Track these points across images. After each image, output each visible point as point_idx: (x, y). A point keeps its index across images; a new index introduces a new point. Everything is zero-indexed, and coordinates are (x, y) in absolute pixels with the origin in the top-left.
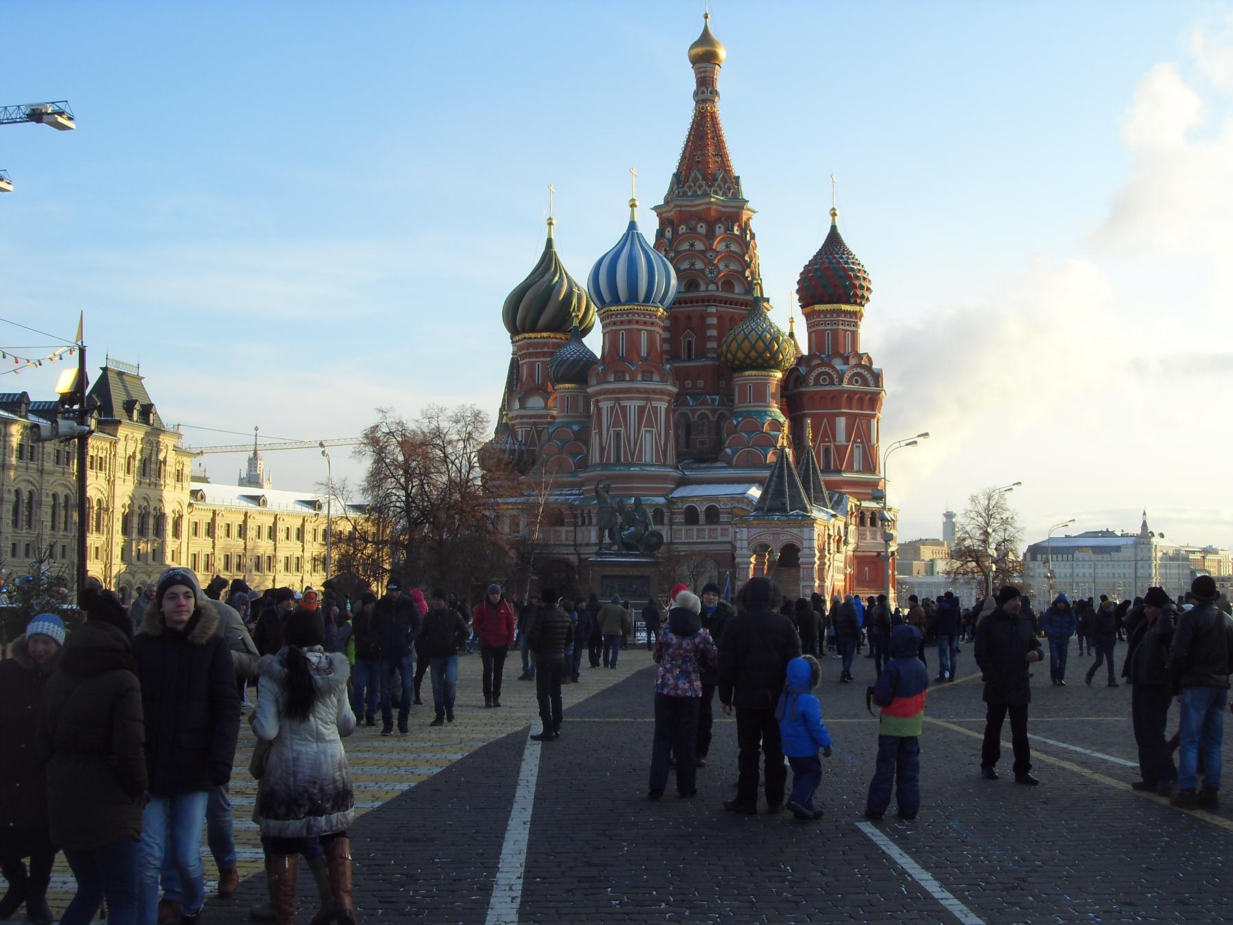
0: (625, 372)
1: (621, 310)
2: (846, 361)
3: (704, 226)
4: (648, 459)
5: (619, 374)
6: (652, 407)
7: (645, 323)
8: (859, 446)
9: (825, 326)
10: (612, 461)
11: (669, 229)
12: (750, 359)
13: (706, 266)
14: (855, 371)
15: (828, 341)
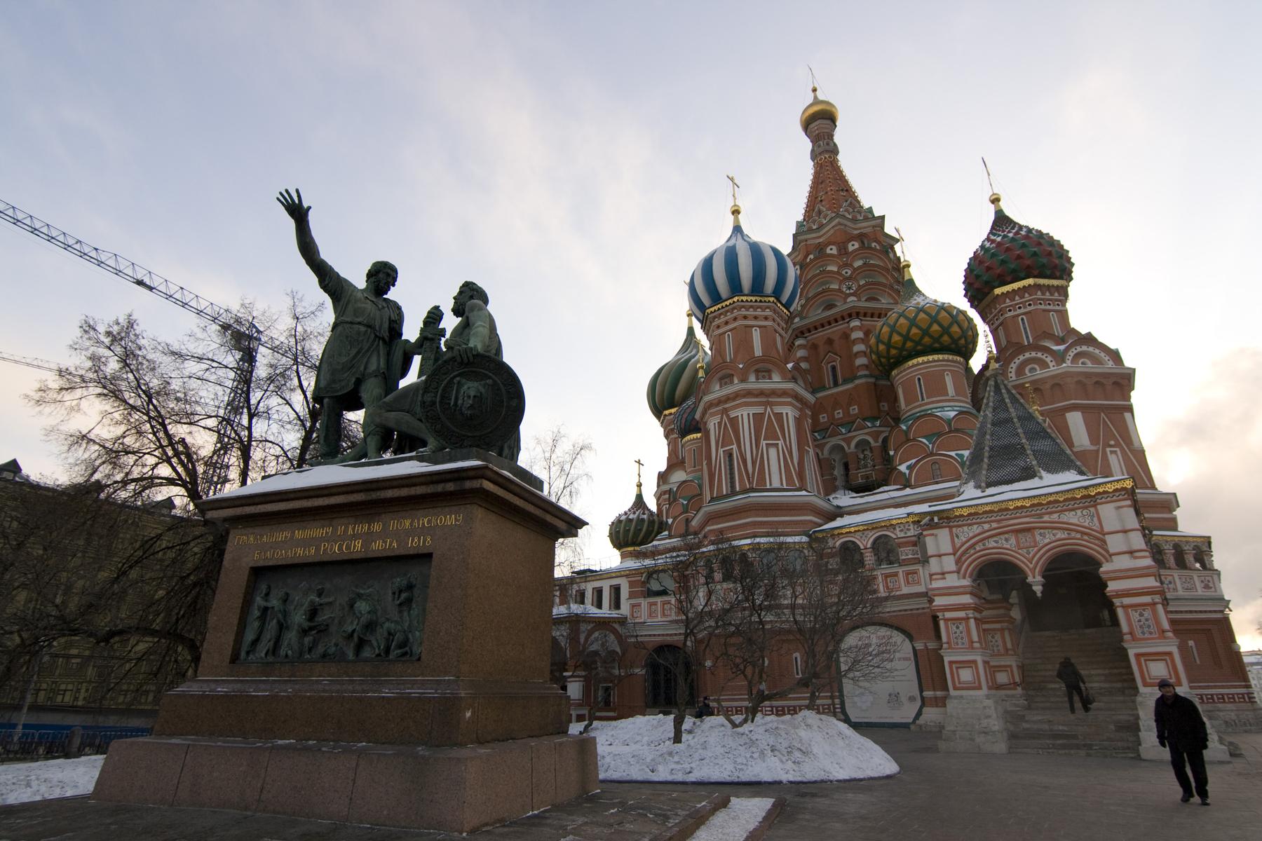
0: (733, 375)
1: (723, 307)
2: (1061, 341)
3: (834, 247)
4: (776, 484)
5: (726, 380)
6: (772, 412)
7: (756, 318)
8: (1115, 452)
9: (1015, 310)
10: (725, 493)
11: (798, 267)
12: (912, 341)
13: (841, 282)
14: (1079, 349)
15: (1025, 328)
